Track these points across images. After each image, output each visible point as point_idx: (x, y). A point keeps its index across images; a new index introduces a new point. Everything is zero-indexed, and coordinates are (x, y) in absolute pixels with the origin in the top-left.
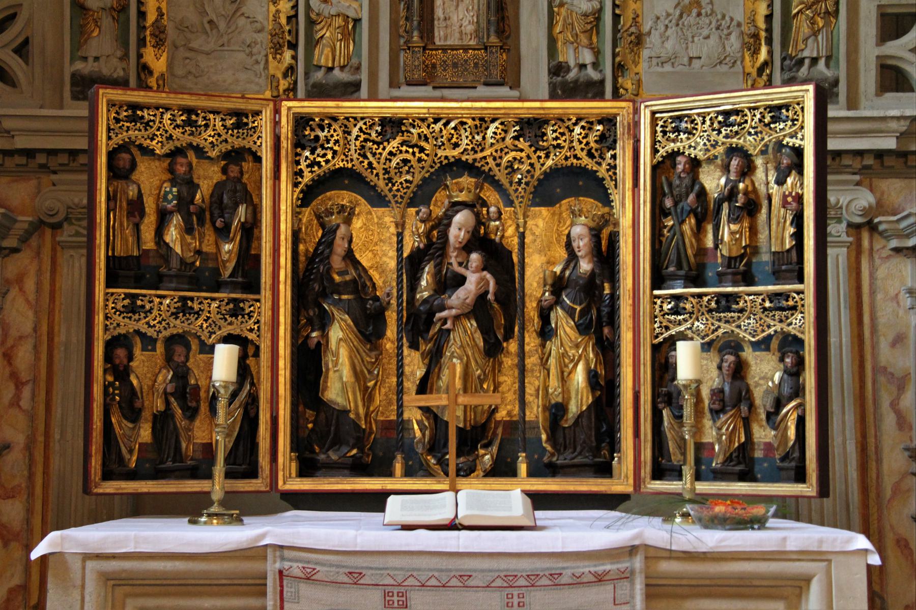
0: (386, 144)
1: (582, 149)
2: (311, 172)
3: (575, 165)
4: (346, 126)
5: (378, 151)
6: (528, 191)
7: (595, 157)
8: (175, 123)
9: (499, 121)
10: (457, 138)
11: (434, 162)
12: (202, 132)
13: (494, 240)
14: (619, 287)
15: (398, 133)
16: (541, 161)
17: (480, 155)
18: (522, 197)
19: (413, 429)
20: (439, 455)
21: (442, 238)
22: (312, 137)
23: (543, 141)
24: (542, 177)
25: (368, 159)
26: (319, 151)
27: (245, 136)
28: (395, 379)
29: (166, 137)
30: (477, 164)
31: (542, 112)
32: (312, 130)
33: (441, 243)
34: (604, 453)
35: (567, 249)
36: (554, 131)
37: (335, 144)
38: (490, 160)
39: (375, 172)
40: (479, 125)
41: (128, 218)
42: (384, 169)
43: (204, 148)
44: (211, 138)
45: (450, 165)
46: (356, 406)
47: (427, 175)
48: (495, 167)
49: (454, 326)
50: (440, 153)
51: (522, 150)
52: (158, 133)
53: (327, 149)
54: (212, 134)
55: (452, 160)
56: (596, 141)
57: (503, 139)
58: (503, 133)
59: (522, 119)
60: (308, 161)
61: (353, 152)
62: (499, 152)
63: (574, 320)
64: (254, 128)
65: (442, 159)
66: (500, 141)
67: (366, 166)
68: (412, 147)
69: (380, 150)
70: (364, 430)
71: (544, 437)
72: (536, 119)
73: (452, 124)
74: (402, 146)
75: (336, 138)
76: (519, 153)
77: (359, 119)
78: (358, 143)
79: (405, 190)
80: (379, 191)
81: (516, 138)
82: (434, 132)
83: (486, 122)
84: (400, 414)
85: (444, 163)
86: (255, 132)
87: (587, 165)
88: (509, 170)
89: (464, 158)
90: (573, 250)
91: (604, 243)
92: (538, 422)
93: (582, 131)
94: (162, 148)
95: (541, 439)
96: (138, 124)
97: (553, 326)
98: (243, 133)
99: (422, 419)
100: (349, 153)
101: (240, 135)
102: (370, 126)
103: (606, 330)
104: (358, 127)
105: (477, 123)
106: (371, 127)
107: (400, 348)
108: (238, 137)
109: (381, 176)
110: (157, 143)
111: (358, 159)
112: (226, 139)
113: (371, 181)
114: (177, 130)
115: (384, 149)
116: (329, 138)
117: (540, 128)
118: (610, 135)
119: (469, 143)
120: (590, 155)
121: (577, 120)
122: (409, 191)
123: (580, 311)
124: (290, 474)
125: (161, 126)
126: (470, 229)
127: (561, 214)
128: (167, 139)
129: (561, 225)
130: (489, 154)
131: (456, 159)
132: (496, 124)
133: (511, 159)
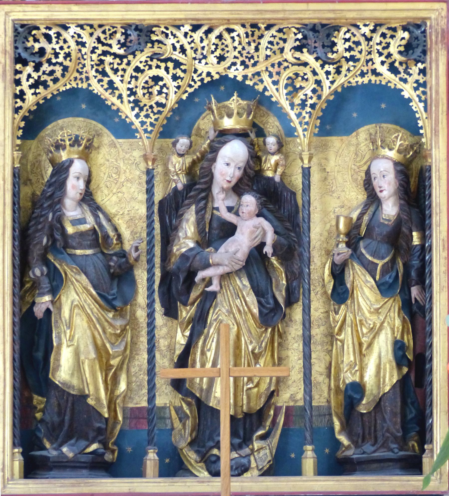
0: (130, 57)
1: (383, 63)
2: (35, 94)
3: (373, 82)
4: (79, 36)
5: (120, 67)
6: (314, 117)
7: (400, 73)
9: (276, 28)
10: (223, 50)
11: (193, 80)
13: (272, 179)
14: (431, 236)
15: (147, 43)
16: (330, 77)
17: (250, 71)
18: (307, 123)
19: (171, 418)
20: (203, 450)
21: (207, 176)
22: (36, 50)
23: (333, 52)
24: (332, 98)
25: (108, 76)
26: (46, 67)
28: (146, 356)
30: (248, 82)
31: (331, 15)
32: (36, 40)
33: (206, 183)
34: (413, 446)
36: (347, 40)
37: (65, 58)
38: (265, 76)
39: (117, 93)
40: (250, 33)
42: (129, 89)
45: (213, 83)
46: (97, 389)
47: (184, 97)
48: (271, 85)
49: (221, 287)
50: (202, 68)
51: (305, 64)
53: (55, 64)
55: (216, 77)
56: (400, 53)
57: (282, 50)
58: (281, 42)
59: (306, 25)
60: (31, 81)
61: (88, 68)
62: (276, 66)
63: (374, 279)
65: (204, 75)
66: (278, 52)
67: (106, 86)
68: (166, 61)
69: (124, 66)
70: (107, 420)
71: (337, 425)
72: (323, 26)
73: (216, 32)
74: (152, 60)
75: (67, 50)
76: (302, 67)
77: (96, 26)
78: (94, 57)
79: (156, 116)
80: (123, 117)
81: (298, 49)
82: (192, 41)
83: (259, 29)
84: (151, 399)
85: (205, 82)
88: (290, 88)
89: (231, 74)
90: (373, 189)
91: (413, 181)
92: (329, 408)
93: (382, 39)
95: (332, 429)
97: (349, 286)
99: (182, 406)
100: (85, 69)
102: (111, 35)
103: (415, 291)
104: (95, 36)
105: (249, 30)
106: (112, 35)
107: (151, 315)
109: (125, 99)
111: (95, 77)
113: (113, 104)
115: (129, 64)
116: (58, 50)
117: (328, 36)
118: (418, 45)
119: (238, 55)
120: (393, 69)
121: (376, 26)
122: (162, 117)
123: (383, 266)
124: (12, 474)
126: (242, 165)
127: (358, 145)
129: (358, 159)
130: (264, 69)
131: (221, 77)
132: (273, 31)
133: (291, 75)
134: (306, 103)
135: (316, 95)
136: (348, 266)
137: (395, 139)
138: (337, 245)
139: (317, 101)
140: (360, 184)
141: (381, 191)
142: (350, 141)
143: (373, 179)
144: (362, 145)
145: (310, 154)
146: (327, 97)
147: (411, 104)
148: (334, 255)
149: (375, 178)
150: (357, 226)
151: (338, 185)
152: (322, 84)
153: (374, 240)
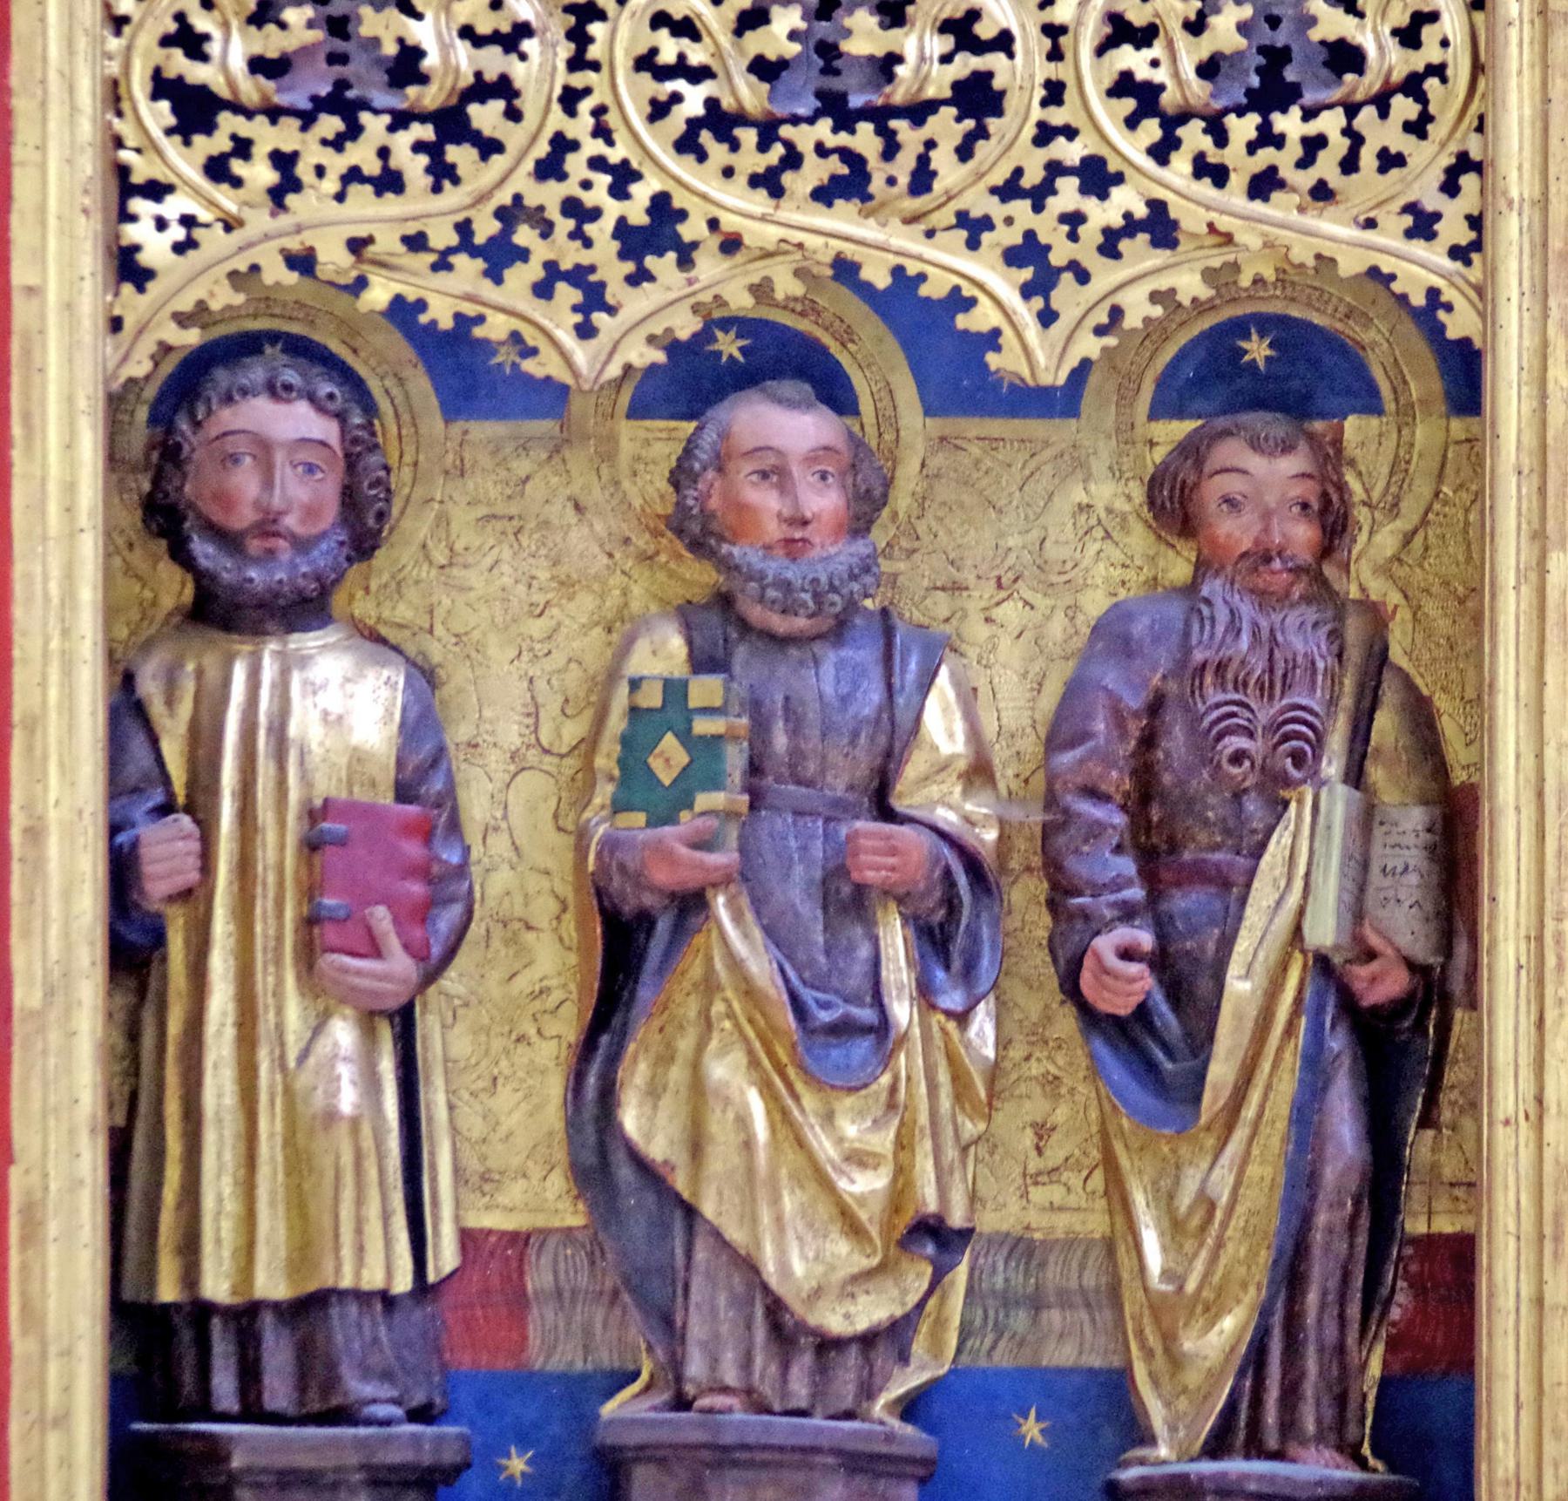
8: (694, 100)
12: (942, 159)
27: (1327, 166)
29: (622, 229)
41: (308, 955)
43: (959, 302)
44: (1021, 208)
52: (549, 195)
54: (1034, 176)
64: (1413, 86)
86: (1417, 128)
94: (585, 331)
96: (374, 125)
98: (1314, 145)
101: (1285, 159)
108: (1264, 185)
110: (543, 290)
112: (1157, 207)
114: (718, 152)
125: (580, 127)
128: (633, 242)
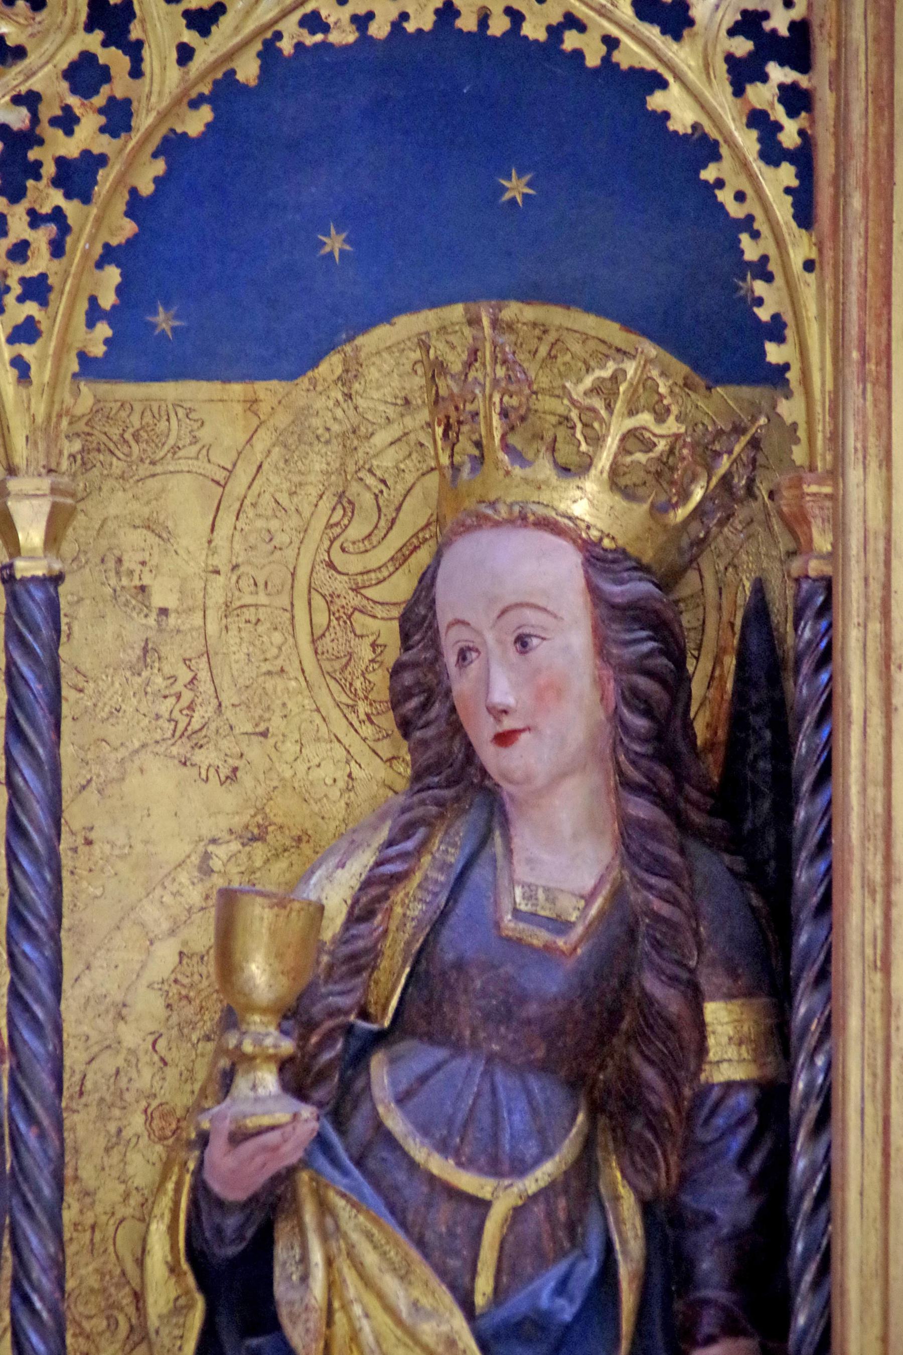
35: (406, 726)
63: (466, 1304)
87: (572, 22)
129: (356, 531)
134: (33, 155)
135: (99, 100)
136: (297, 1213)
137: (598, 404)
138: (227, 1080)
139: (103, 144)
140: (370, 688)
141: (504, 739)
142: (305, 412)
143: (451, 658)
144: (381, 438)
145: (54, 490)
146: (163, 116)
147: (709, 174)
148: (204, 1139)
149: (463, 656)
150: (353, 957)
151: (229, 697)
152: (135, 33)
153: (458, 1049)
